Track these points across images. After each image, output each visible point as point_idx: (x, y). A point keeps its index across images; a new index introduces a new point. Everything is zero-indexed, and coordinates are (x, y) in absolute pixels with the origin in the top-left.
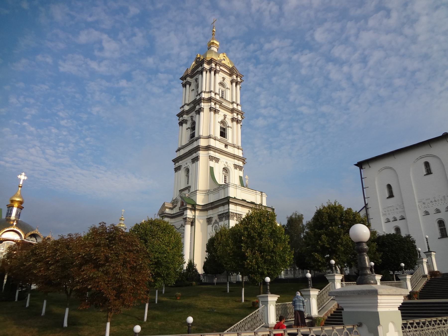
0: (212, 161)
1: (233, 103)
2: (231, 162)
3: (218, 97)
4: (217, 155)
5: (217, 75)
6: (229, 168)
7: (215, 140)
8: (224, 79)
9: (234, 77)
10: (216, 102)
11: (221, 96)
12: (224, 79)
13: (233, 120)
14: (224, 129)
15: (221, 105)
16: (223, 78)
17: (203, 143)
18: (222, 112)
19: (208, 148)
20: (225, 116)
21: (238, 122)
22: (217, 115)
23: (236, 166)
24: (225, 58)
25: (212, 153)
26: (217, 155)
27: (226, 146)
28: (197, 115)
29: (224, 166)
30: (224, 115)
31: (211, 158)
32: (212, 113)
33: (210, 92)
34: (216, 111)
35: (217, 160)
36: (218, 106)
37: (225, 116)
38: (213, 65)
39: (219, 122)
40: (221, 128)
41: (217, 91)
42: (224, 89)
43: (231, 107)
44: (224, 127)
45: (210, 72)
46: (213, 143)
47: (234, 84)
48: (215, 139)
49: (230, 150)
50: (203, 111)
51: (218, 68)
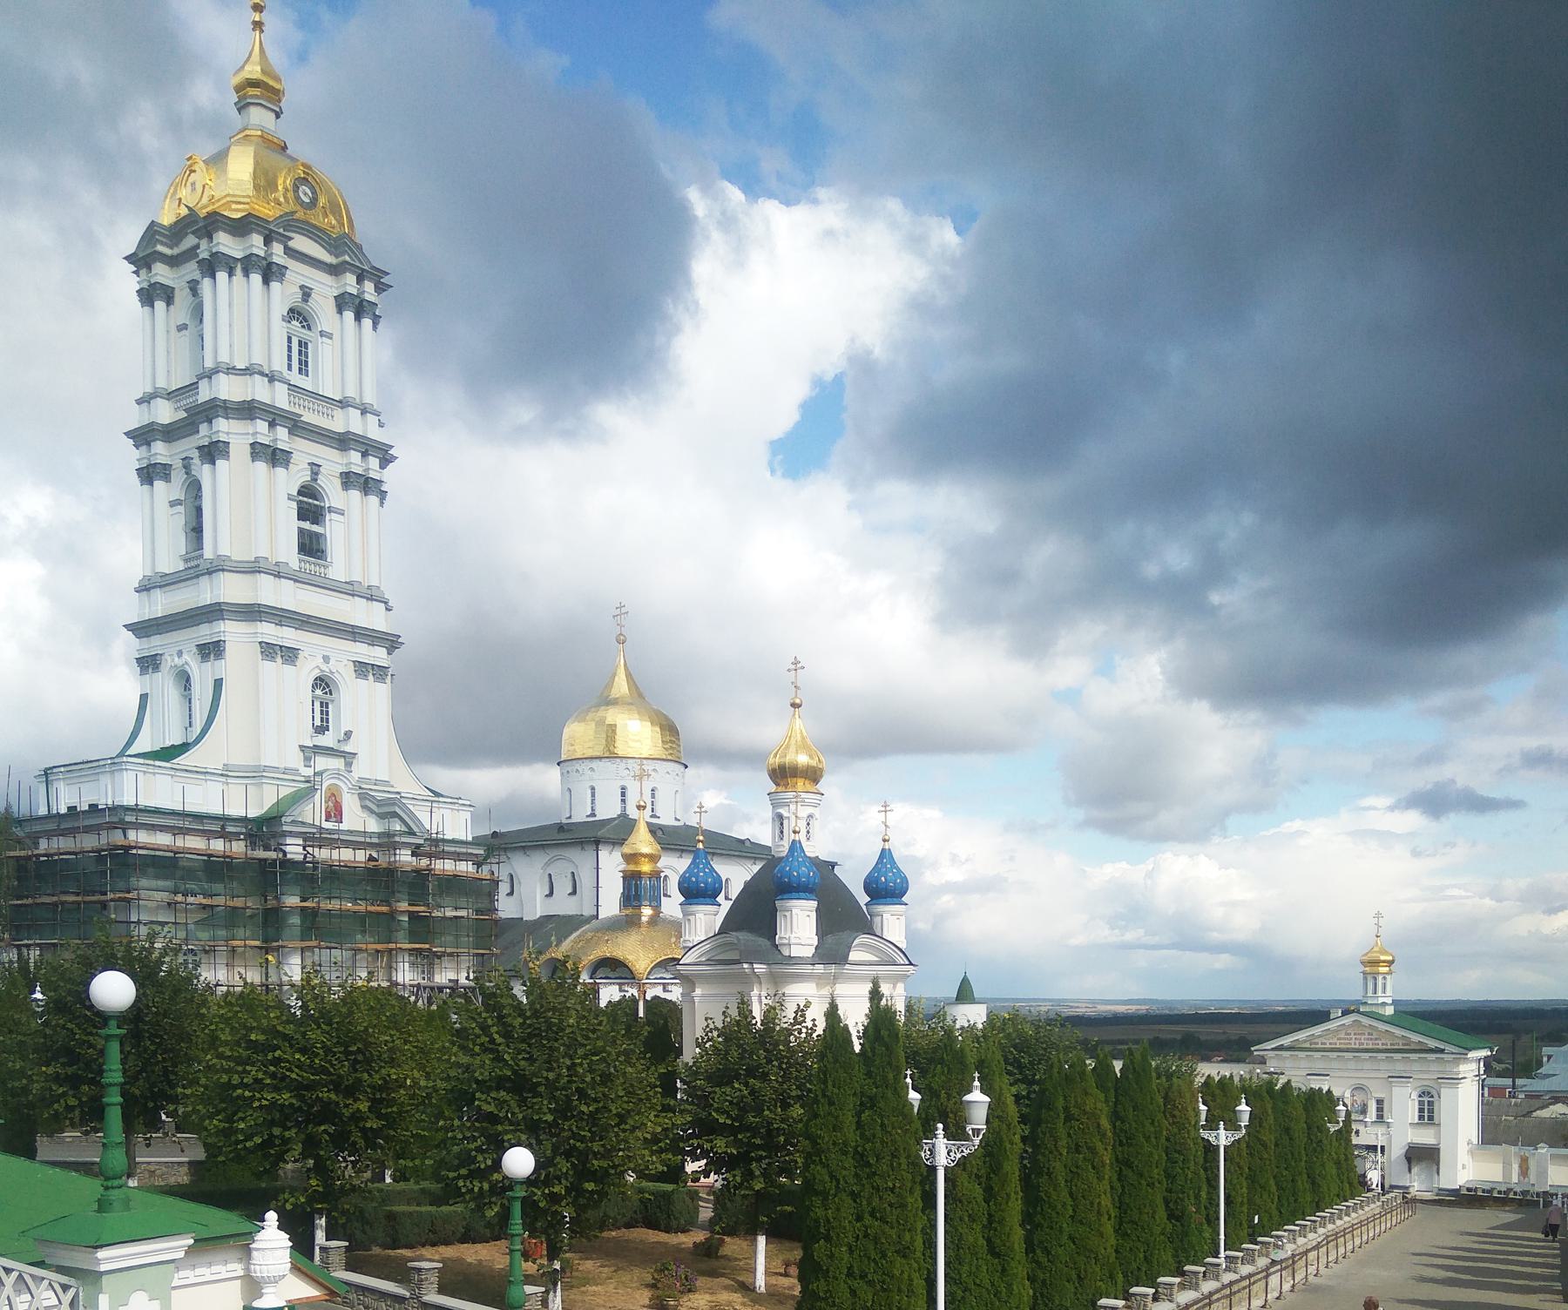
0: (273, 659)
3: (280, 398)
5: (275, 285)
7: (278, 575)
10: (275, 417)
16: (302, 287)
17: (231, 589)
18: (304, 451)
19: (252, 612)
22: (280, 471)
25: (269, 631)
26: (287, 636)
28: (207, 467)
29: (316, 673)
31: (269, 650)
32: (261, 466)
33: (248, 371)
34: (275, 457)
35: (290, 655)
38: (256, 242)
41: (279, 364)
45: (246, 274)
46: (270, 592)
50: (225, 454)
51: (277, 248)
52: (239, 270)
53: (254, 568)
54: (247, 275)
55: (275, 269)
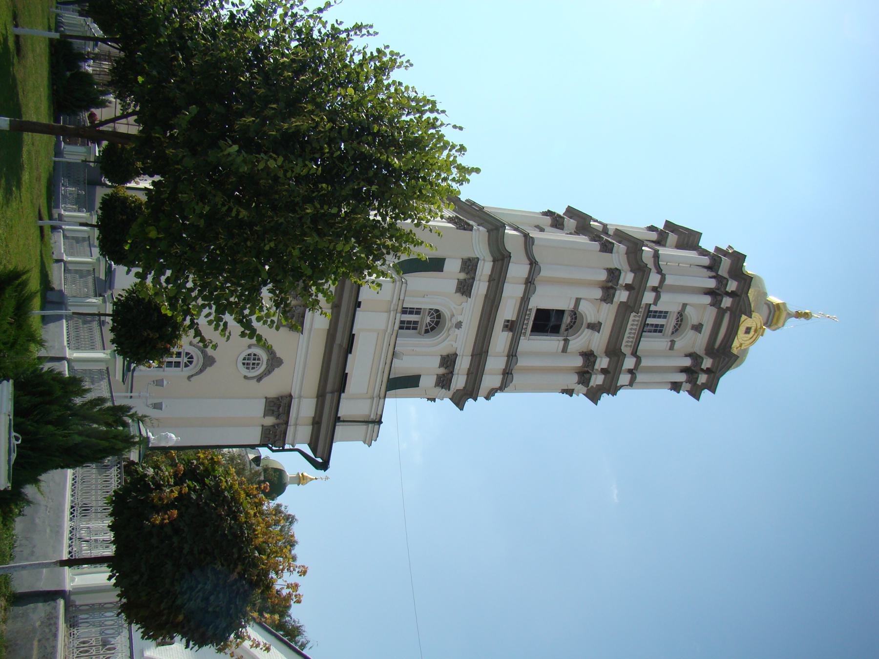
0: (462, 270)
1: (634, 354)
2: (460, 341)
3: (648, 297)
4: (480, 288)
5: (707, 299)
6: (444, 334)
8: (698, 328)
9: (707, 363)
10: (637, 290)
11: (653, 308)
12: (698, 328)
13: (589, 356)
14: (555, 330)
15: (626, 309)
20: (595, 327)
21: (584, 376)
22: (598, 293)
23: (448, 361)
24: (752, 332)
25: (485, 268)
26: (480, 288)
27: (510, 326)
30: (600, 324)
31: (470, 265)
32: (603, 276)
35: (465, 288)
36: (622, 296)
37: (595, 327)
38: (732, 286)
39: (578, 301)
40: (561, 313)
42: (669, 329)
43: (626, 349)
44: (563, 327)
46: (518, 270)
47: (687, 362)
48: (530, 283)
49: (500, 340)
51: (727, 302)
52: (713, 274)
53: (533, 264)
54: (710, 277)
55: (719, 298)
